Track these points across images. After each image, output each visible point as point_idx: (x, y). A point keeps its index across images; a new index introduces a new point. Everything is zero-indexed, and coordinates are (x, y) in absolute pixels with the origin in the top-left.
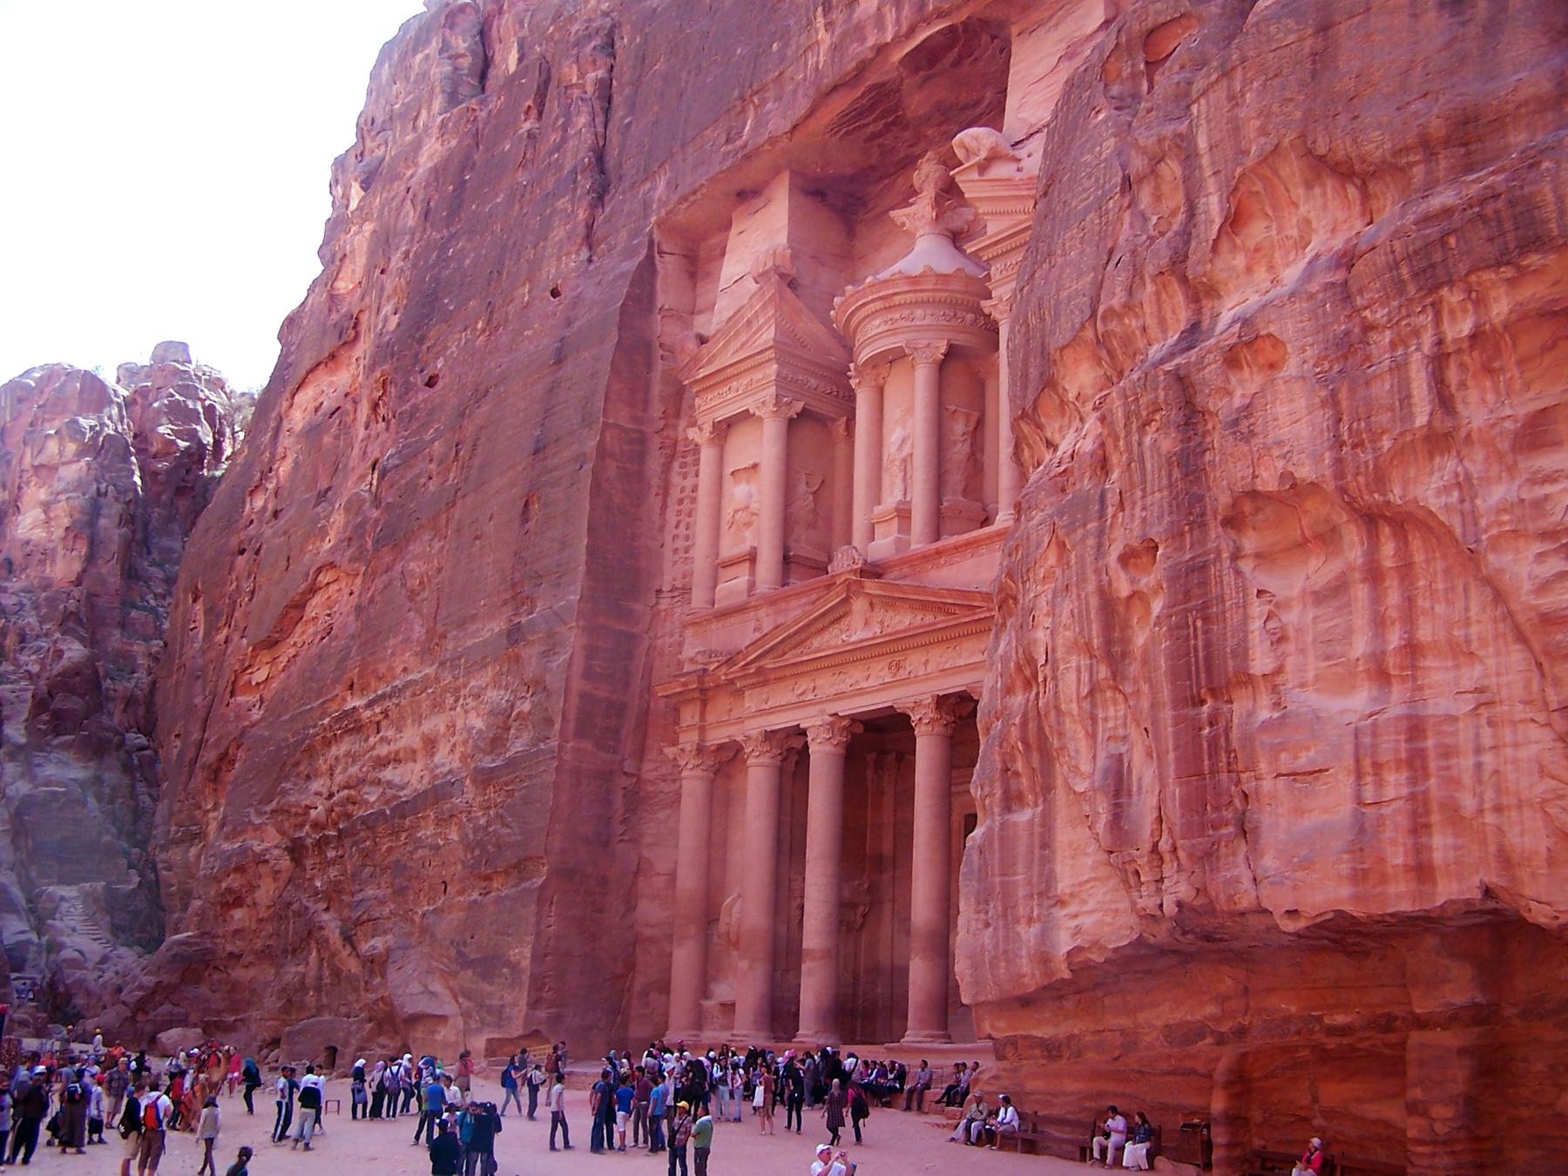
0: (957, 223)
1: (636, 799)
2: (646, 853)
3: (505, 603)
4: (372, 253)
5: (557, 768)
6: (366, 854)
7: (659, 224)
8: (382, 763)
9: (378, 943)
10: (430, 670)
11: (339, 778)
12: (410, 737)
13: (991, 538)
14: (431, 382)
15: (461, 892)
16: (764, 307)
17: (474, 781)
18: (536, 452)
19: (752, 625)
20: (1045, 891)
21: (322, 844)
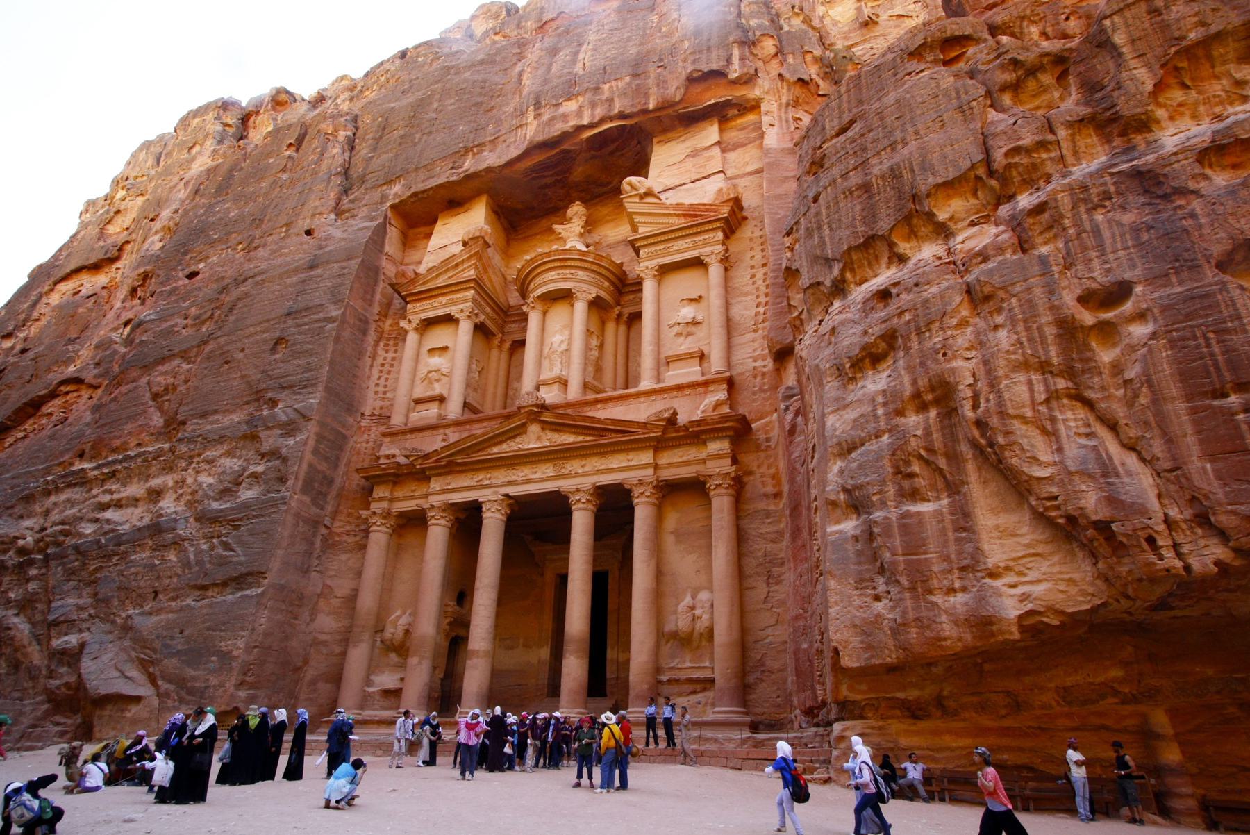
0: (590, 241)
1: (329, 545)
2: (329, 582)
3: (247, 403)
4: (143, 209)
5: (286, 511)
6: (71, 573)
7: (393, 207)
8: (104, 507)
9: (72, 640)
10: (167, 446)
11: (55, 516)
12: (135, 489)
13: (638, 395)
14: (192, 275)
15: (174, 599)
16: (469, 258)
17: (197, 520)
18: (288, 314)
19: (441, 437)
20: (971, 566)
21: (22, 568)
